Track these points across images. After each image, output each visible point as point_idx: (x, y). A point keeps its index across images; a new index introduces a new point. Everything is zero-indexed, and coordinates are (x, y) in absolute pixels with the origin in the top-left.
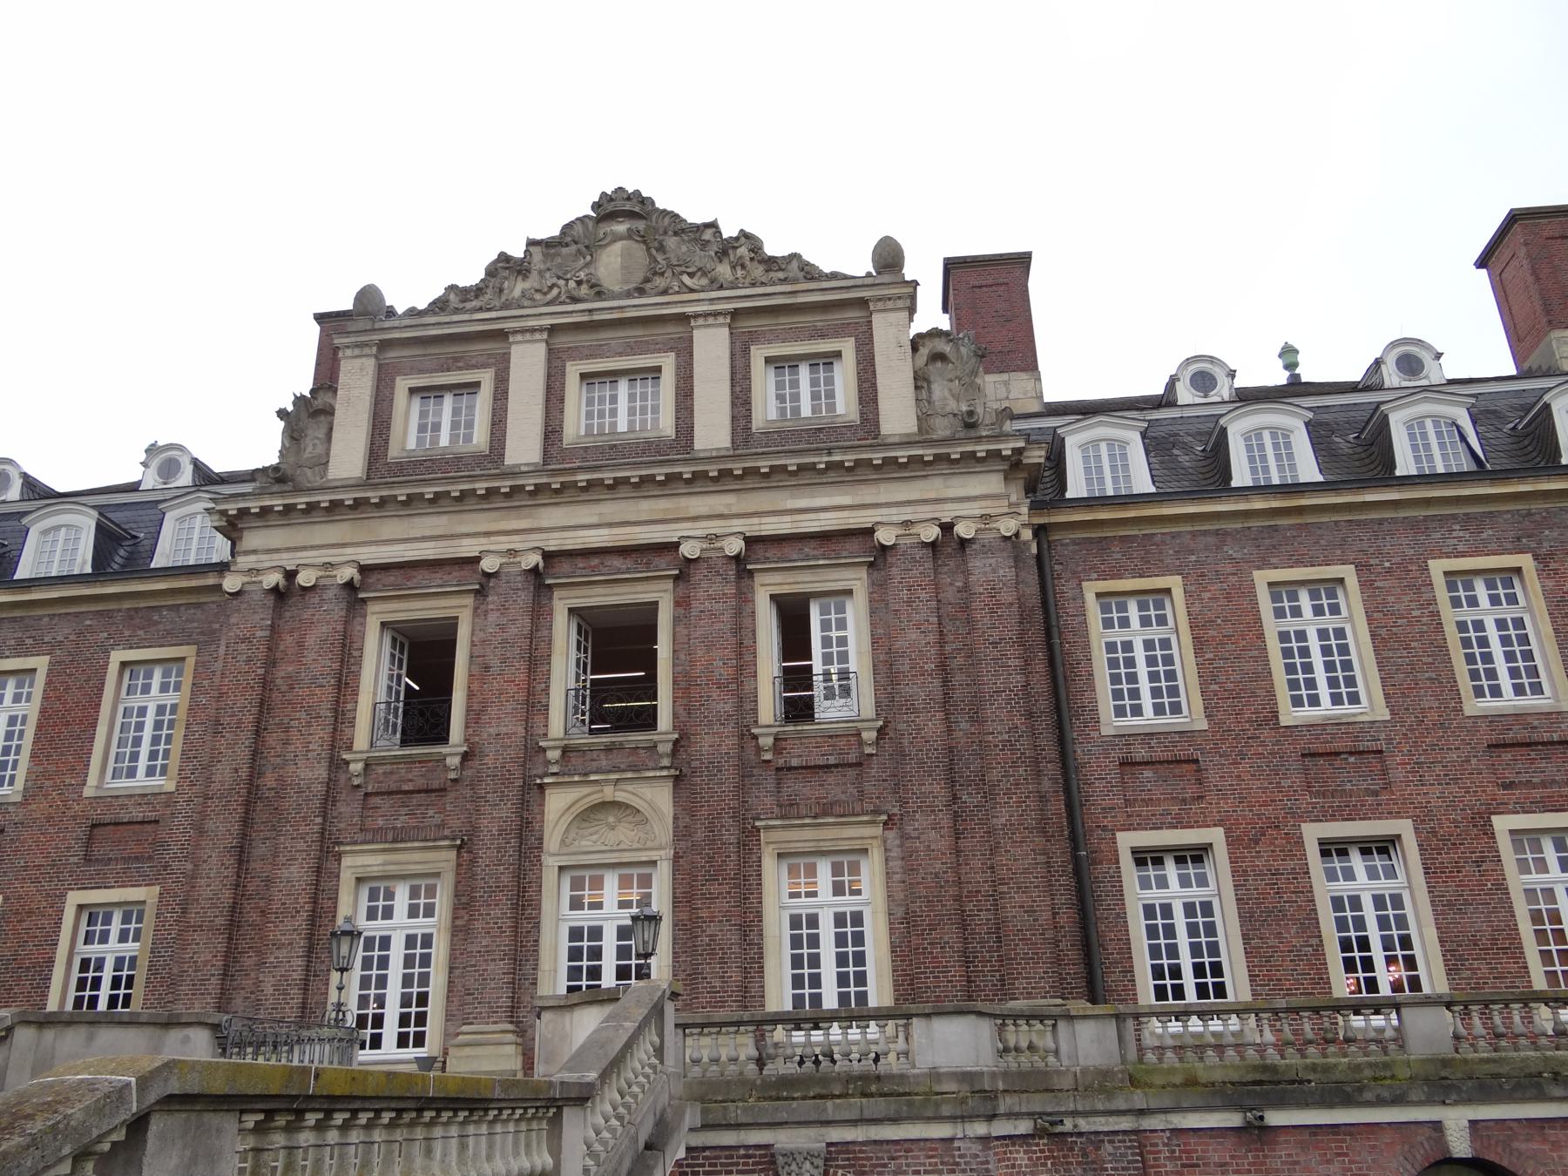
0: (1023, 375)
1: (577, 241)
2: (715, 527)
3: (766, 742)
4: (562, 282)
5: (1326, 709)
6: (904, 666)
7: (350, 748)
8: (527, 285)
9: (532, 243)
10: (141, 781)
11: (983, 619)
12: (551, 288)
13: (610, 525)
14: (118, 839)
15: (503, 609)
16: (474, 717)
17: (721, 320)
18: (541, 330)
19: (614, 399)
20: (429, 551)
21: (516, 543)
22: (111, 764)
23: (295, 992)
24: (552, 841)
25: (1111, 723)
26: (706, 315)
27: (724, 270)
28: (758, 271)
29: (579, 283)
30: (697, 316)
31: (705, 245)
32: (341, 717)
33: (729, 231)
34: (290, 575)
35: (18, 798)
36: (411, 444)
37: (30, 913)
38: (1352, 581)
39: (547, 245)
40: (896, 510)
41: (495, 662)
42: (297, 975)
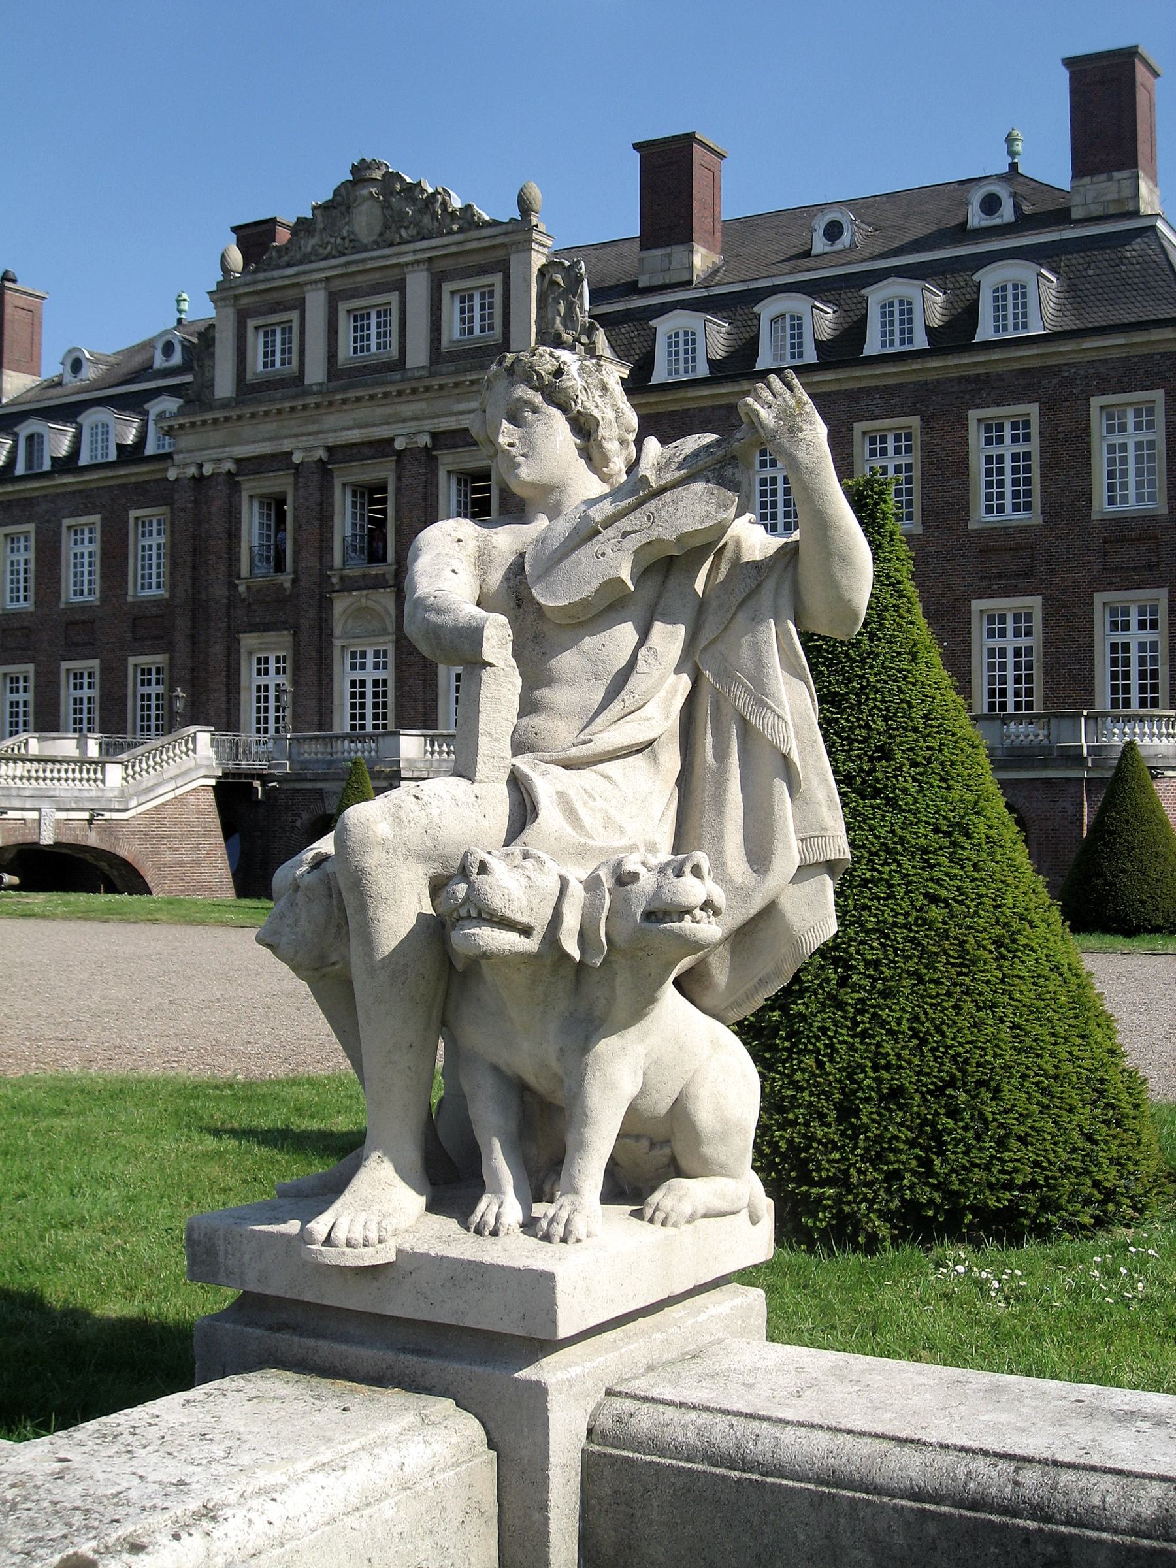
0: (681, 248)
1: (339, 205)
2: (413, 426)
4: (332, 240)
7: (239, 578)
8: (312, 242)
9: (314, 208)
12: (328, 243)
13: (360, 427)
17: (422, 266)
18: (321, 281)
22: (140, 581)
23: (223, 715)
24: (337, 631)
26: (412, 263)
27: (426, 220)
28: (448, 220)
29: (343, 239)
30: (407, 264)
31: (414, 200)
32: (233, 557)
35: (98, 603)
36: (260, 368)
37: (113, 669)
41: (303, 522)
42: (224, 706)
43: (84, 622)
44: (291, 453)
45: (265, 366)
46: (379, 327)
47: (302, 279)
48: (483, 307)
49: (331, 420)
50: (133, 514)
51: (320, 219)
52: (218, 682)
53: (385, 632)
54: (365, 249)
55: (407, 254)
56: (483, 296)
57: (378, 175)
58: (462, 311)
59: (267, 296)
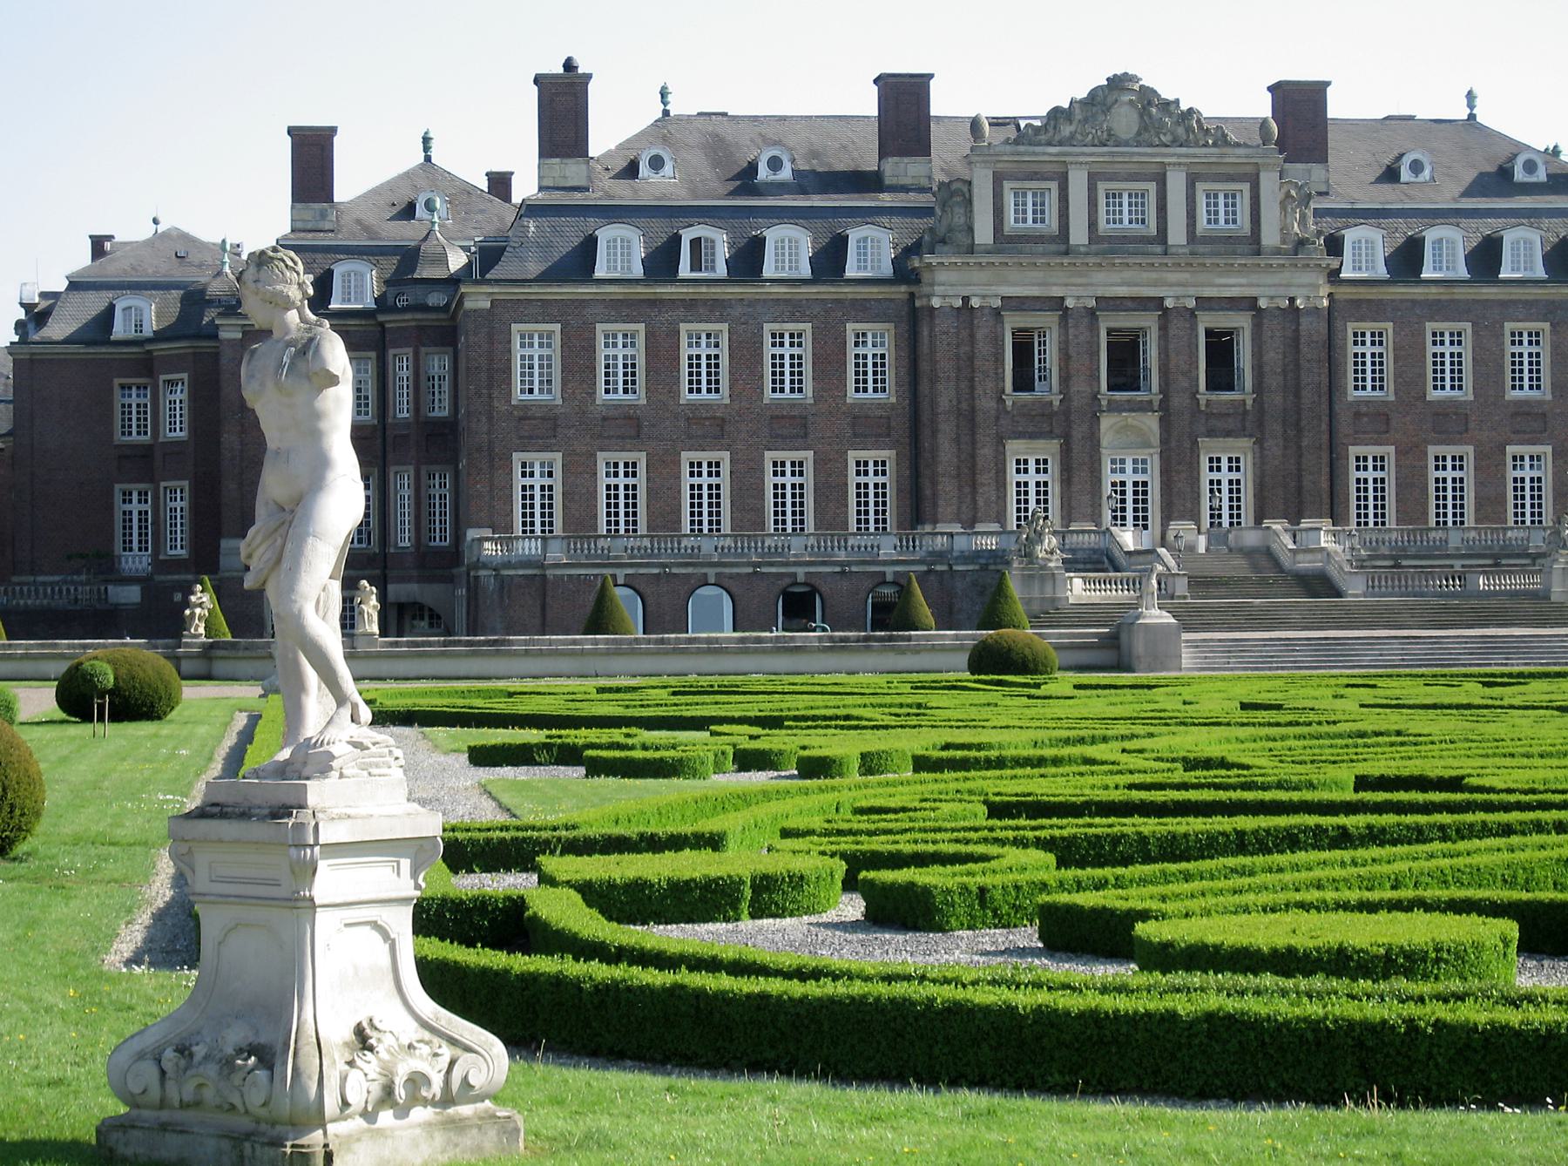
2: (1180, 291)
3: (1203, 402)
5: (1448, 392)
6: (1267, 369)
7: (1003, 392)
10: (870, 394)
11: (1304, 349)
13: (1129, 285)
14: (866, 428)
15: (1076, 326)
16: (1065, 379)
19: (1121, 205)
20: (1035, 291)
21: (1080, 291)
24: (1104, 442)
25: (1353, 395)
28: (1200, 136)
33: (1184, 107)
34: (966, 299)
38: (1469, 331)
39: (1082, 102)
40: (1269, 288)
41: (1072, 352)
43: (794, 417)
44: (1062, 299)
45: (1016, 220)
46: (1130, 205)
47: (1068, 159)
48: (1226, 205)
49: (1099, 277)
50: (850, 326)
51: (1077, 111)
52: (985, 478)
53: (1147, 445)
54: (1127, 144)
55: (1172, 155)
56: (1226, 196)
57: (1136, 87)
58: (1208, 205)
59: (1024, 165)
